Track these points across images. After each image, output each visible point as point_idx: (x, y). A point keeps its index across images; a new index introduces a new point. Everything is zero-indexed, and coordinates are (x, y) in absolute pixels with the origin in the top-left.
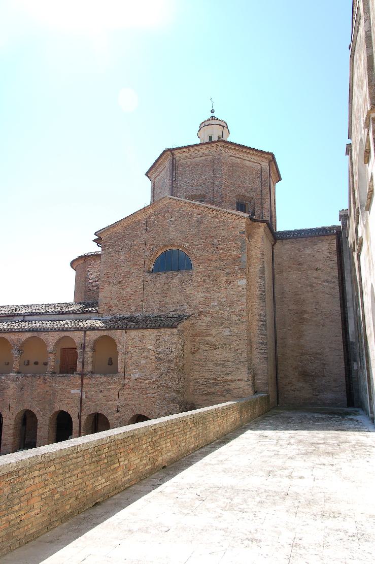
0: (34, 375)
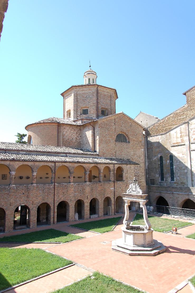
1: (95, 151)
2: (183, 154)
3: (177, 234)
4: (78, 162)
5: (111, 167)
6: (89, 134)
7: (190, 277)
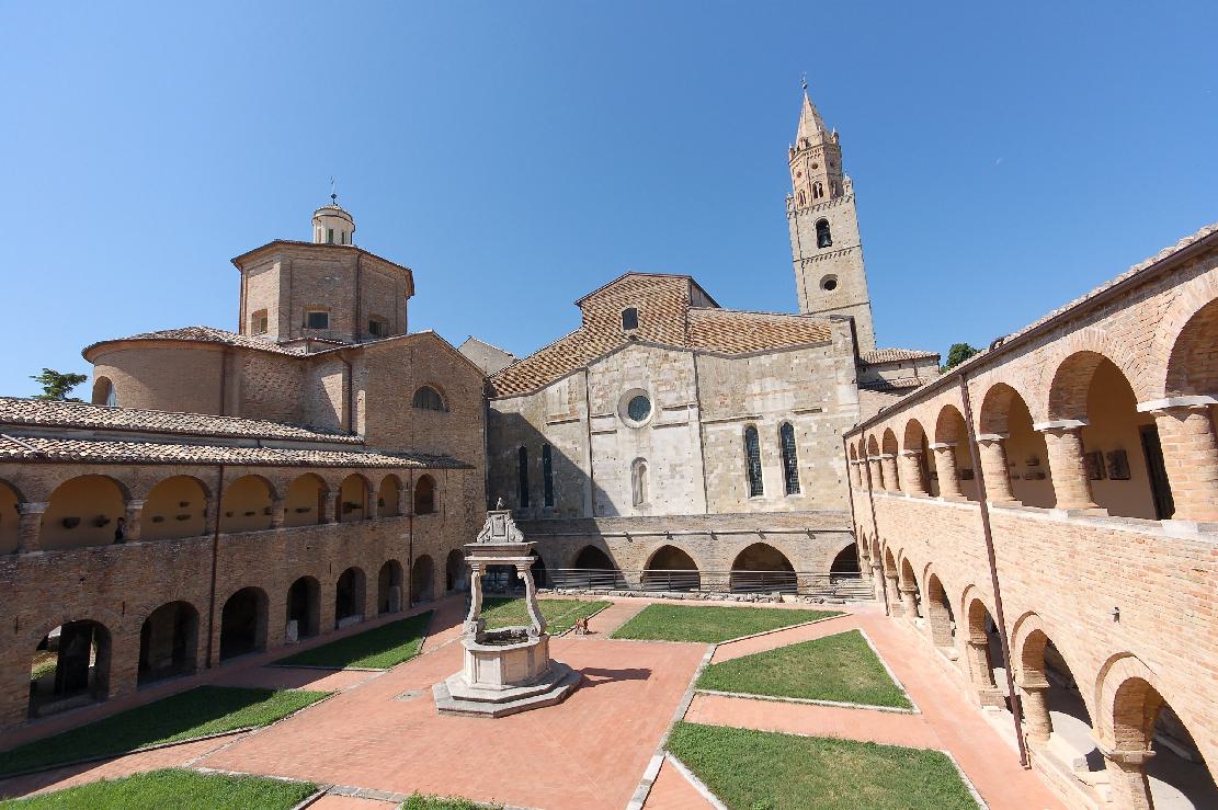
1: (354, 434)
2: (574, 443)
3: (589, 633)
4: (305, 464)
5: (404, 476)
6: (333, 384)
7: (663, 741)
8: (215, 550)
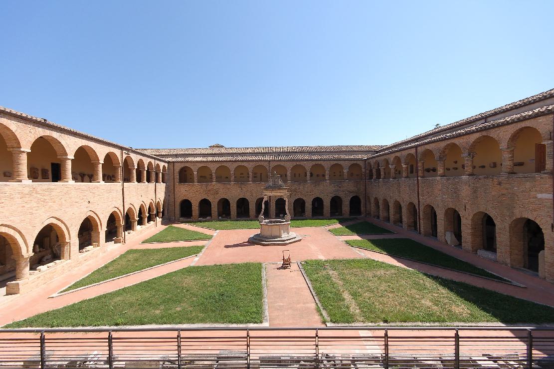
0: (487, 178)
8: (418, 185)
